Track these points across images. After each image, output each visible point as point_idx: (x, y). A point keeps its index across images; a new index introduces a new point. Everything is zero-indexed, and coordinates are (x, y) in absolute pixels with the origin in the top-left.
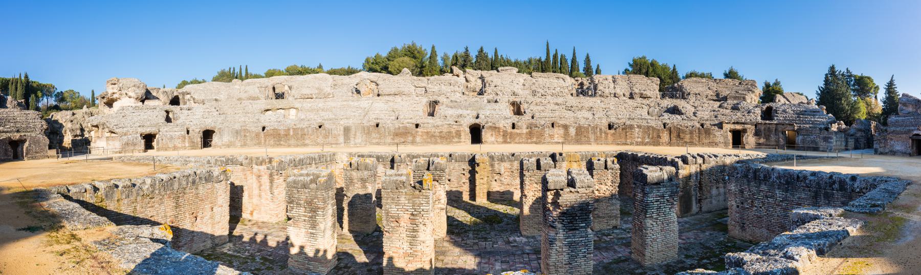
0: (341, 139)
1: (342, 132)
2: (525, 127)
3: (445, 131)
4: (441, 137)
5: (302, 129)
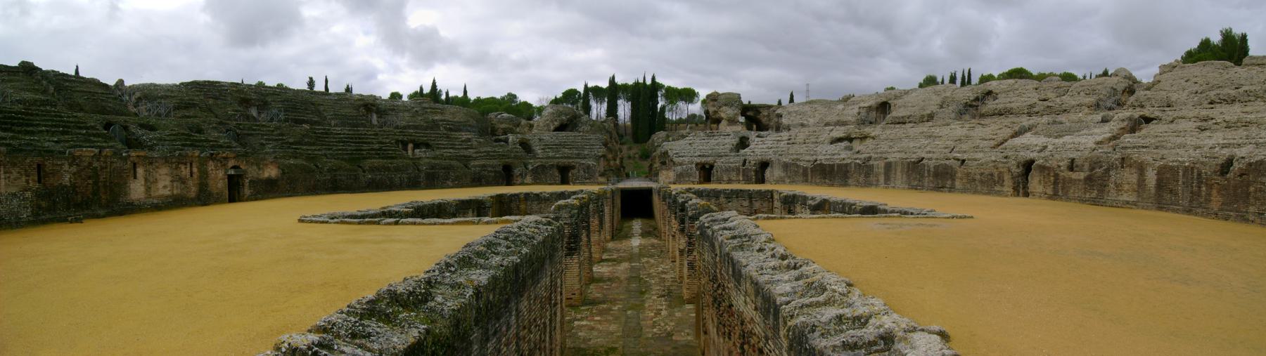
0: (882, 179)
1: (882, 171)
2: (1087, 166)
3: (987, 172)
4: (982, 182)
5: (846, 165)
